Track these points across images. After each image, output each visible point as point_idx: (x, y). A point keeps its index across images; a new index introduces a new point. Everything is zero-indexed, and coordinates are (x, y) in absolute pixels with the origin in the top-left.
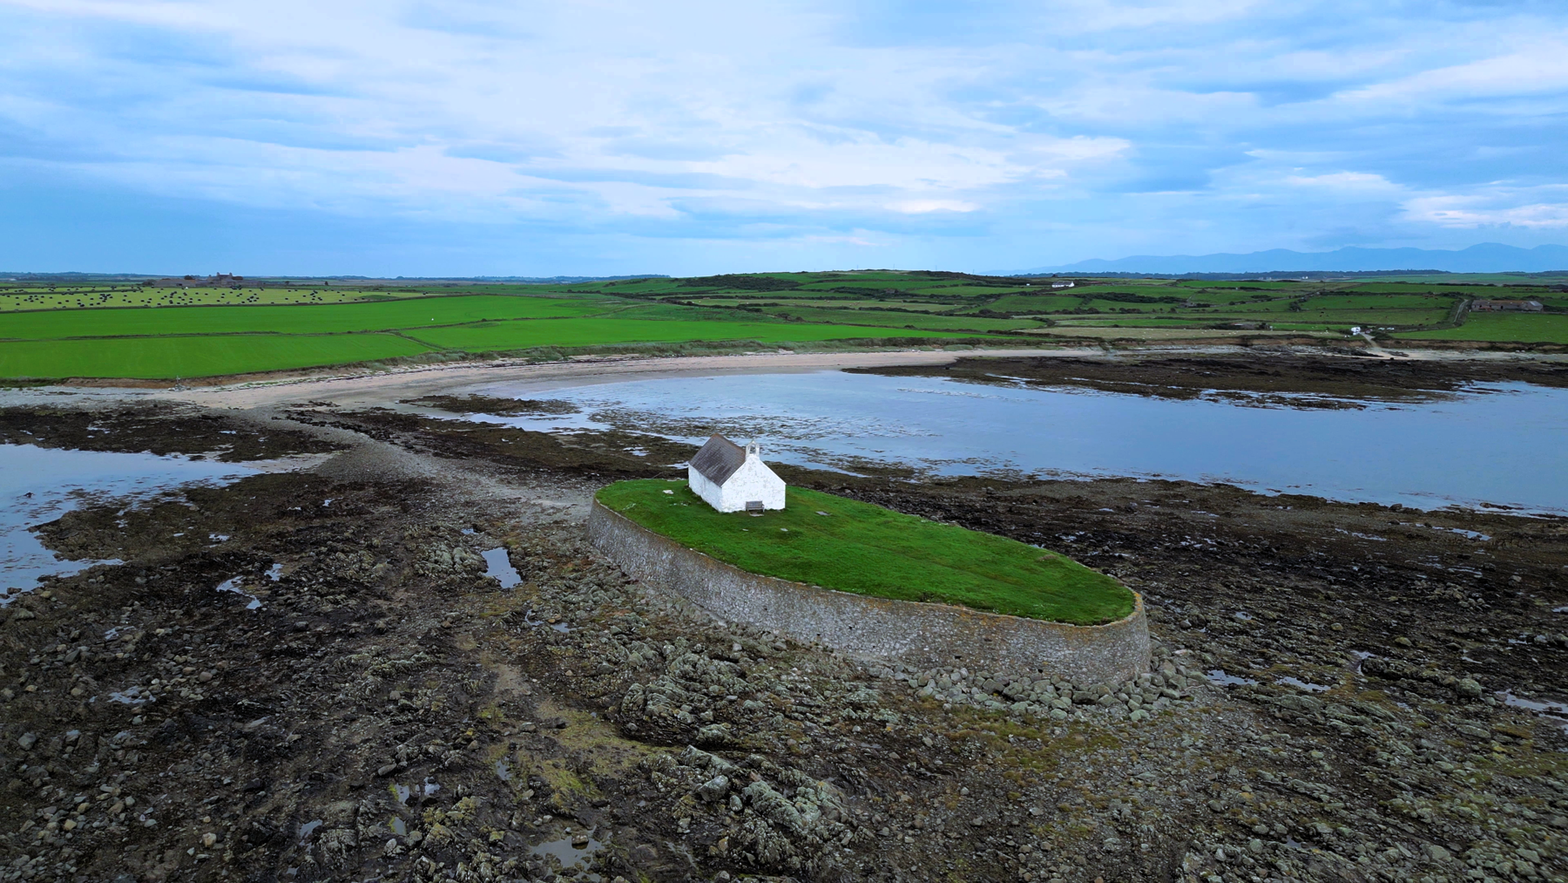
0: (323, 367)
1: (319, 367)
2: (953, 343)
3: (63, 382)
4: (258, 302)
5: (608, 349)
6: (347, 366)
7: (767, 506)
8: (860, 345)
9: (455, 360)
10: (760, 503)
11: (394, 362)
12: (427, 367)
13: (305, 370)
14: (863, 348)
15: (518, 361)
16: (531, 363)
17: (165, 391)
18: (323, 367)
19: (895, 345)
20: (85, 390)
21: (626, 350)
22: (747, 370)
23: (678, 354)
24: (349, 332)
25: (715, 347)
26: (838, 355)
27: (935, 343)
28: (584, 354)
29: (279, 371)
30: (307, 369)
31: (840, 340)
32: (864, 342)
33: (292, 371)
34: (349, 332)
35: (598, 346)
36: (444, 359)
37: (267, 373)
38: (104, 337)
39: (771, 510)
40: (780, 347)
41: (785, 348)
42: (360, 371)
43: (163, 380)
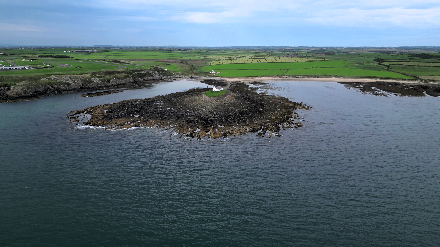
2: (384, 78)
3: (219, 77)
5: (305, 75)
6: (255, 76)
8: (361, 77)
9: (275, 76)
11: (263, 76)
12: (268, 77)
13: (248, 77)
14: (361, 78)
15: (285, 77)
19: (369, 78)
21: (308, 76)
22: (315, 81)
23: (318, 77)
24: (281, 70)
25: (328, 76)
26: (355, 79)
27: (379, 78)
28: (299, 76)
31: (357, 76)
32: (362, 77)
34: (281, 70)
35: (303, 75)
36: (272, 76)
37: (242, 77)
40: (342, 77)
41: (343, 77)
42: (256, 77)
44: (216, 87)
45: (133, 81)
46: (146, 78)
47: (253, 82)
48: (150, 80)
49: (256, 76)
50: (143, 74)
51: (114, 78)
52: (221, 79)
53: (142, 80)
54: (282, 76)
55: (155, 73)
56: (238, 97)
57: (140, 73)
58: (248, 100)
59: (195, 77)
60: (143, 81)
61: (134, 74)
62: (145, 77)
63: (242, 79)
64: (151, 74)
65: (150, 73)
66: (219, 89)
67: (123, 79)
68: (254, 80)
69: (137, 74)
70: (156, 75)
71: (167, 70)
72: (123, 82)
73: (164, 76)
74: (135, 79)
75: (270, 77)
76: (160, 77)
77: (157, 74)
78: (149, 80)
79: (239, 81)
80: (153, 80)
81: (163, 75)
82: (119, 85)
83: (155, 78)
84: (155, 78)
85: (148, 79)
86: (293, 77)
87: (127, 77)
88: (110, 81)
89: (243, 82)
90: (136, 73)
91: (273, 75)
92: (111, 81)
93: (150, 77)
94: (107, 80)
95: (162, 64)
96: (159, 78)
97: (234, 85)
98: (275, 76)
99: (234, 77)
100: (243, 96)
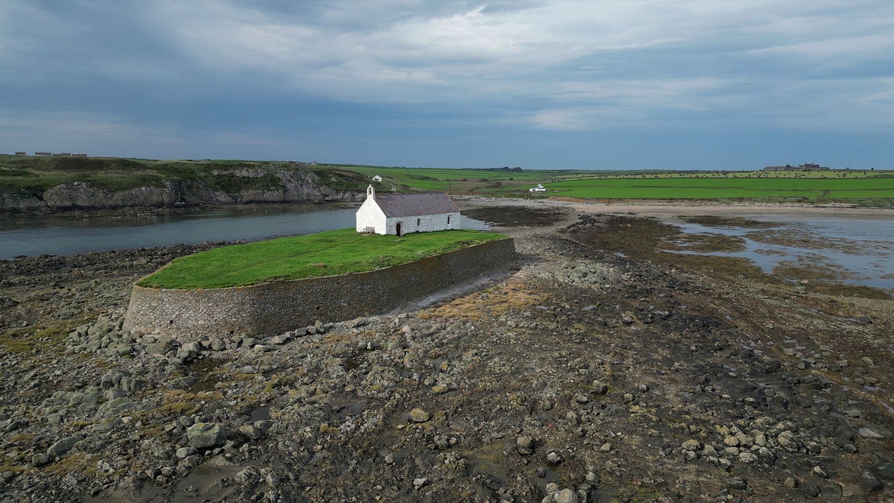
0: (685, 199)
1: (682, 199)
4: (802, 177)
7: (377, 232)
10: (373, 229)
11: (741, 200)
12: (764, 204)
15: (843, 205)
16: (854, 207)
17: (581, 204)
18: (685, 199)
20: (552, 201)
24: (795, 190)
29: (653, 199)
30: (673, 199)
33: (662, 199)
34: (795, 190)
36: (782, 200)
37: (645, 199)
38: (647, 187)
39: (379, 234)
42: (709, 203)
43: (582, 198)
44: (377, 200)
45: (166, 199)
46: (248, 194)
47: (700, 216)
48: (267, 202)
49: (710, 200)
50: (244, 177)
51: (76, 183)
52: (552, 205)
53: (229, 199)
54: (829, 203)
55: (303, 180)
56: (579, 296)
57: (232, 176)
58: (706, 348)
59: (459, 200)
60: (228, 203)
61: (203, 174)
62: (247, 190)
63: (644, 207)
64: (279, 179)
65: (278, 175)
66: (414, 219)
67: (123, 190)
68: (701, 211)
69: (218, 175)
70: (302, 185)
71: (380, 180)
72: (118, 197)
73: (337, 193)
74: (194, 195)
75: (770, 204)
76: (318, 194)
77: (310, 181)
78: (259, 202)
79: (630, 213)
80: (284, 202)
81: (338, 188)
82: (75, 207)
83: (293, 195)
84: (296, 198)
85: (257, 199)
86: (881, 207)
87: (145, 181)
88: (43, 191)
89: (650, 215)
90: (215, 173)
91: (785, 198)
92: (46, 195)
93: (270, 190)
94: (28, 188)
95: (408, 175)
96: (312, 198)
97: (596, 224)
98: (794, 199)
99: (609, 201)
100: (633, 292)
